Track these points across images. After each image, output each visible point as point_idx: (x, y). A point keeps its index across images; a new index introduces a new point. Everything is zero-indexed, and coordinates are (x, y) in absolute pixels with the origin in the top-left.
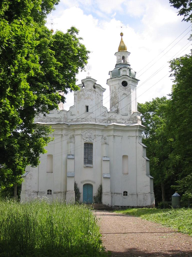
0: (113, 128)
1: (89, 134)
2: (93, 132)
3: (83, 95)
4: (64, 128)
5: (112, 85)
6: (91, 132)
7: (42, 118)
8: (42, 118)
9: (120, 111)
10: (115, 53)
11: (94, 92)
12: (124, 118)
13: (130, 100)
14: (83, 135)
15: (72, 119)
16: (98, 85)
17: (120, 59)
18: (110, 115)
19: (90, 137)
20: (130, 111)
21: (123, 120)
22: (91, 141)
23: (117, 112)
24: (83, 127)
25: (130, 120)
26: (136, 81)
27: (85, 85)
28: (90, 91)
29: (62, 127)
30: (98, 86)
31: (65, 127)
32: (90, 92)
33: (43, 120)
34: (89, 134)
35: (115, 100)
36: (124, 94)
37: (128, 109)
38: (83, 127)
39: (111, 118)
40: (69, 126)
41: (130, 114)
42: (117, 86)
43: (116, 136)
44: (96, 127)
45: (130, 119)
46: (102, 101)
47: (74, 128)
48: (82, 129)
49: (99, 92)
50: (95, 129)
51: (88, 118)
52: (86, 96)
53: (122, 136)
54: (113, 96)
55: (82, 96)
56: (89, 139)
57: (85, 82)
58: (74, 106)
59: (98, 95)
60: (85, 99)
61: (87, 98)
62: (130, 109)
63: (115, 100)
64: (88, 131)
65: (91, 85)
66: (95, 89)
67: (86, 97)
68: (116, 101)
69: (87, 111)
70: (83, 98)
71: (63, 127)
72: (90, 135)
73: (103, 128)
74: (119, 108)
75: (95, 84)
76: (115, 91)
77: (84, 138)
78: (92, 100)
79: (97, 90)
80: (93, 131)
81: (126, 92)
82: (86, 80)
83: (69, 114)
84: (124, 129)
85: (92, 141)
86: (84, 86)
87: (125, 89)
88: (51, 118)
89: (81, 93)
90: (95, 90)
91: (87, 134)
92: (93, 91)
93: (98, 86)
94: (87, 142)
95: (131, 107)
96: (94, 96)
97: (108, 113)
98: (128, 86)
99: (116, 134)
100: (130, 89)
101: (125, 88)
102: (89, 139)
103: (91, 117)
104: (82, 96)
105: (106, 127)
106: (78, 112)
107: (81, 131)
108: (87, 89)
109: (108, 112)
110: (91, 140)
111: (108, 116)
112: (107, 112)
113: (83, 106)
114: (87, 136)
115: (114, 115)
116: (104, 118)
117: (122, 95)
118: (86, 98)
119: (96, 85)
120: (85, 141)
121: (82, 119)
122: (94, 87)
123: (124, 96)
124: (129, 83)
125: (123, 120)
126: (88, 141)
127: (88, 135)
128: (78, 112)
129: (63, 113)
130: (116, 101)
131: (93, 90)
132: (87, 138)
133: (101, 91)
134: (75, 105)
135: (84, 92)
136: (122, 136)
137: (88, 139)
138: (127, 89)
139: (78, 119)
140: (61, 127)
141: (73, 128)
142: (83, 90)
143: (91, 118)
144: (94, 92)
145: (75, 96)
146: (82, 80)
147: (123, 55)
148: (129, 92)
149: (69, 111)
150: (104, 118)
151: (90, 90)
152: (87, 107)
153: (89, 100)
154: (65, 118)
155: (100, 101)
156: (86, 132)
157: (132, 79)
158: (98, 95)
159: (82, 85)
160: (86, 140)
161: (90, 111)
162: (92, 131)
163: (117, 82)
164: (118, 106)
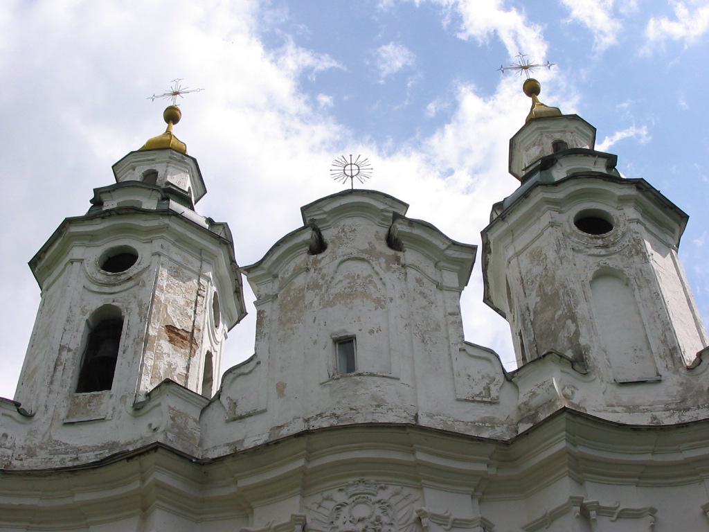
0: (563, 445)
1: (362, 511)
2: (397, 494)
3: (315, 286)
4: (159, 485)
5: (517, 255)
6: (383, 495)
7: (10, 452)
8: (10, 452)
9: (595, 355)
10: (512, 142)
11: (395, 266)
12: (638, 401)
13: (657, 296)
15: (234, 443)
16: (412, 222)
17: (542, 150)
18: (525, 390)
20: (673, 352)
21: (631, 409)
23: (579, 363)
24: (310, 466)
25: (689, 403)
26: (668, 218)
27: (327, 235)
28: (365, 256)
29: (143, 480)
30: (417, 231)
31: (162, 477)
32: (365, 265)
33: (15, 463)
34: (362, 511)
35: (547, 315)
36: (603, 274)
37: (655, 345)
38: (308, 461)
39: (535, 402)
40: (204, 469)
41: (676, 372)
42: (550, 237)
43: (601, 511)
44: (421, 456)
45: (684, 400)
46: (457, 313)
47: (243, 483)
48: (306, 483)
49: (431, 271)
50: (417, 476)
51: (353, 405)
52: (334, 291)
53: (653, 511)
54: (533, 300)
55: (309, 296)
57: (324, 221)
58: (251, 359)
59: (425, 280)
60: (331, 304)
61: (347, 296)
62: (664, 342)
63: (547, 315)
64: (352, 490)
65: (367, 233)
66: (400, 254)
67: (334, 291)
68: (560, 312)
69: (349, 365)
70: (316, 303)
71: (149, 480)
72: (378, 519)
73: (482, 468)
74: (583, 341)
75: (397, 217)
76: (537, 270)
78: (380, 303)
79: (409, 256)
81: (614, 262)
82: (336, 204)
83: (216, 416)
84: (659, 458)
86: (319, 246)
87: (605, 247)
88: (78, 450)
89: (301, 281)
90: (397, 260)
91: (346, 510)
92: (383, 260)
93: (417, 231)
95: (667, 327)
96: (392, 283)
97: (508, 386)
98: (619, 230)
99: (597, 494)
100: (638, 242)
101: (600, 242)
103: (374, 398)
104: (309, 296)
105: (505, 449)
106: (281, 389)
107: (298, 498)
108: (342, 251)
109: (509, 377)
111: (509, 404)
112: (501, 378)
113: (315, 342)
115: (556, 383)
116: (482, 412)
117: (590, 277)
118: (340, 296)
119: (400, 227)
121: (307, 421)
122: (393, 242)
123: (604, 285)
124: (626, 217)
125: (631, 409)
128: (281, 389)
129: (169, 401)
130: (560, 312)
131: (382, 254)
133: (442, 264)
134: (263, 357)
135: (324, 271)
136: (653, 511)
138: (614, 244)
139: (278, 427)
140: (136, 485)
141: (233, 489)
142: (315, 262)
143: (378, 406)
144: (389, 268)
145: (266, 307)
146: (304, 210)
147: (558, 136)
148: (637, 259)
149: (218, 395)
150: (482, 412)
151: (362, 251)
152: (345, 344)
153: (357, 302)
154: (181, 434)
155: (438, 314)
156: (340, 498)
157: (632, 192)
158: (425, 280)
159: (308, 235)
161: (364, 358)
162: (391, 489)
163: (546, 219)
164: (577, 334)
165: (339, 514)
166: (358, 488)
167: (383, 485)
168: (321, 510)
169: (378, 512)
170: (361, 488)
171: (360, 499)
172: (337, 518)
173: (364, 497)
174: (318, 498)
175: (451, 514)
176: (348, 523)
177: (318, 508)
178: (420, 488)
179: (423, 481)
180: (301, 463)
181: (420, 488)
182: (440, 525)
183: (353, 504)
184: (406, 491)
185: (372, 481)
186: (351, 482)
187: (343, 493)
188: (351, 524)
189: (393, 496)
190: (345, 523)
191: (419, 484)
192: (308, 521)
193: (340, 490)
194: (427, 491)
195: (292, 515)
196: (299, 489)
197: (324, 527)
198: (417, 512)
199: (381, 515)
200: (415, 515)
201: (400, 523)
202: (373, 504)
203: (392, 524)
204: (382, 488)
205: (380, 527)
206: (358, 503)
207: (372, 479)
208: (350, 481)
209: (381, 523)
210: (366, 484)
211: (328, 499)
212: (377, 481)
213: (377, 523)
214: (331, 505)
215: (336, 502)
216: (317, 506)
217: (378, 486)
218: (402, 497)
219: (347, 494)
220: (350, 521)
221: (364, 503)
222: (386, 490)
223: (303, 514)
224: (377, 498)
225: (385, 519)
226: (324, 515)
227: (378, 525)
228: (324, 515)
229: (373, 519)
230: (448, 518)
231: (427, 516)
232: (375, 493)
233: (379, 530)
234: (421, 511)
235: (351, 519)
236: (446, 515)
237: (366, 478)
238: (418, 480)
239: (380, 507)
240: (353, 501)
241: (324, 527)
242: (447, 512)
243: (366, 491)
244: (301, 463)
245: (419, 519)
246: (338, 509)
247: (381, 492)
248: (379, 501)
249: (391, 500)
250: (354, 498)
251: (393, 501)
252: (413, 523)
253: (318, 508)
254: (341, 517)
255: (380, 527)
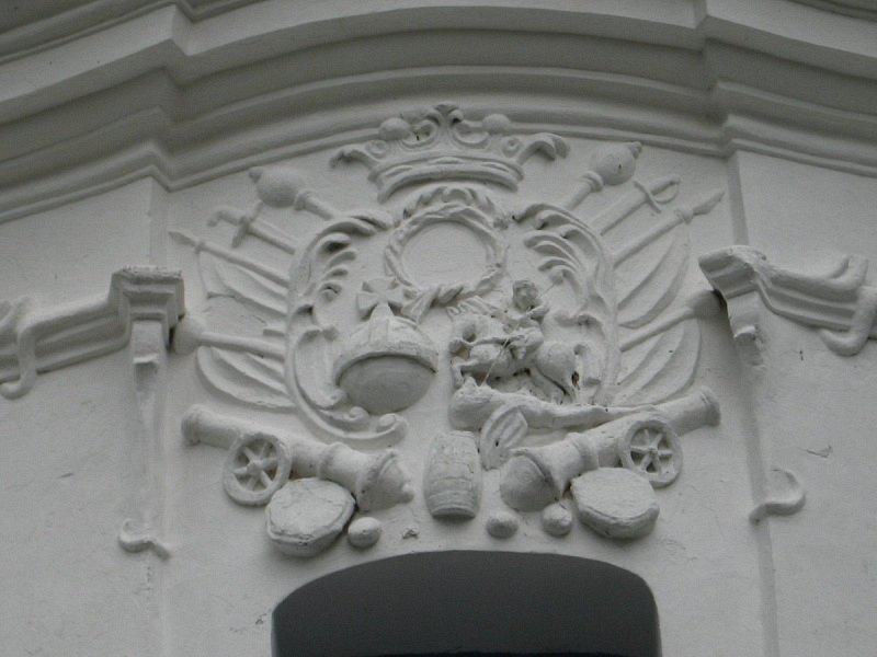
2: (613, 178)
6: (546, 188)
14: (198, 315)
19: (521, 368)
22: (542, 491)
24: (199, 43)
34: (444, 261)
56: (464, 445)
64: (398, 159)
72: (525, 299)
77: (299, 406)
80: (614, 152)
85: (615, 494)
91: (368, 256)
94: (405, 534)
102: (471, 419)
110: (558, 452)
114: (392, 332)
120: (311, 510)
126: (442, 482)
127: (427, 284)
132: (377, 387)
137: (425, 449)
156: (348, 198)
160: (356, 459)
165: (340, 273)
166: (436, 149)
167: (546, 138)
168: (250, 252)
169: (524, 266)
170: (445, 151)
171: (437, 206)
172: (331, 292)
173: (457, 194)
174: (239, 200)
175: (862, 282)
176: (384, 316)
177: (236, 244)
178: (723, 155)
179: (734, 121)
180: (157, 30)
181: (723, 155)
182: (814, 327)
183: (405, 224)
184: (652, 171)
185: (499, 119)
186: (394, 123)
187: (359, 175)
188: (394, 321)
189: (595, 188)
190: (367, 315)
191: (714, 133)
192: (193, 304)
193: (349, 160)
194: (750, 167)
195: (118, 278)
196: (150, 148)
197: (268, 333)
198: (708, 266)
199: (541, 281)
200: (698, 284)
201: (625, 316)
202: (501, 225)
203: (587, 323)
204: (541, 152)
205: (532, 334)
206: (431, 222)
207: (498, 109)
208: (393, 114)
209: (539, 319)
210: (468, 131)
211: (281, 199)
212: (517, 117)
213: (517, 316)
214: (303, 233)
215: (326, 216)
216: (231, 231)
217: (526, 141)
218: (638, 196)
219: (374, 178)
220: (395, 309)
221: (457, 221)
222: (559, 161)
223: (170, 268)
224: (519, 203)
225: (556, 301)
226: (269, 276)
227: (523, 324)
228: (269, 276)
229: (502, 297)
230: (851, 295)
231: (755, 289)
232: (509, 175)
233: (533, 348)
234: (728, 260)
235: (397, 297)
236: (845, 280)
237: (462, 105)
238: (713, 116)
239: (530, 244)
240: (407, 214)
241: (268, 333)
242: (845, 268)
243: (464, 166)
244: (157, 30)
245: (715, 307)
246: (334, 247)
247: (533, 168)
248: (530, 213)
249: (578, 214)
250: (410, 198)
251: (590, 218)
252: (687, 317)
253: (236, 244)
254: (350, 287)
255: (532, 334)
